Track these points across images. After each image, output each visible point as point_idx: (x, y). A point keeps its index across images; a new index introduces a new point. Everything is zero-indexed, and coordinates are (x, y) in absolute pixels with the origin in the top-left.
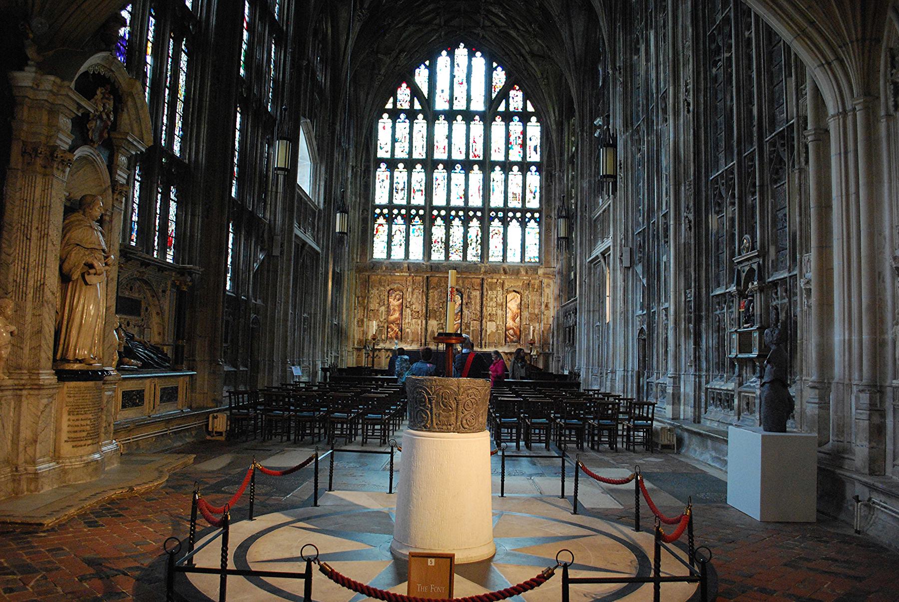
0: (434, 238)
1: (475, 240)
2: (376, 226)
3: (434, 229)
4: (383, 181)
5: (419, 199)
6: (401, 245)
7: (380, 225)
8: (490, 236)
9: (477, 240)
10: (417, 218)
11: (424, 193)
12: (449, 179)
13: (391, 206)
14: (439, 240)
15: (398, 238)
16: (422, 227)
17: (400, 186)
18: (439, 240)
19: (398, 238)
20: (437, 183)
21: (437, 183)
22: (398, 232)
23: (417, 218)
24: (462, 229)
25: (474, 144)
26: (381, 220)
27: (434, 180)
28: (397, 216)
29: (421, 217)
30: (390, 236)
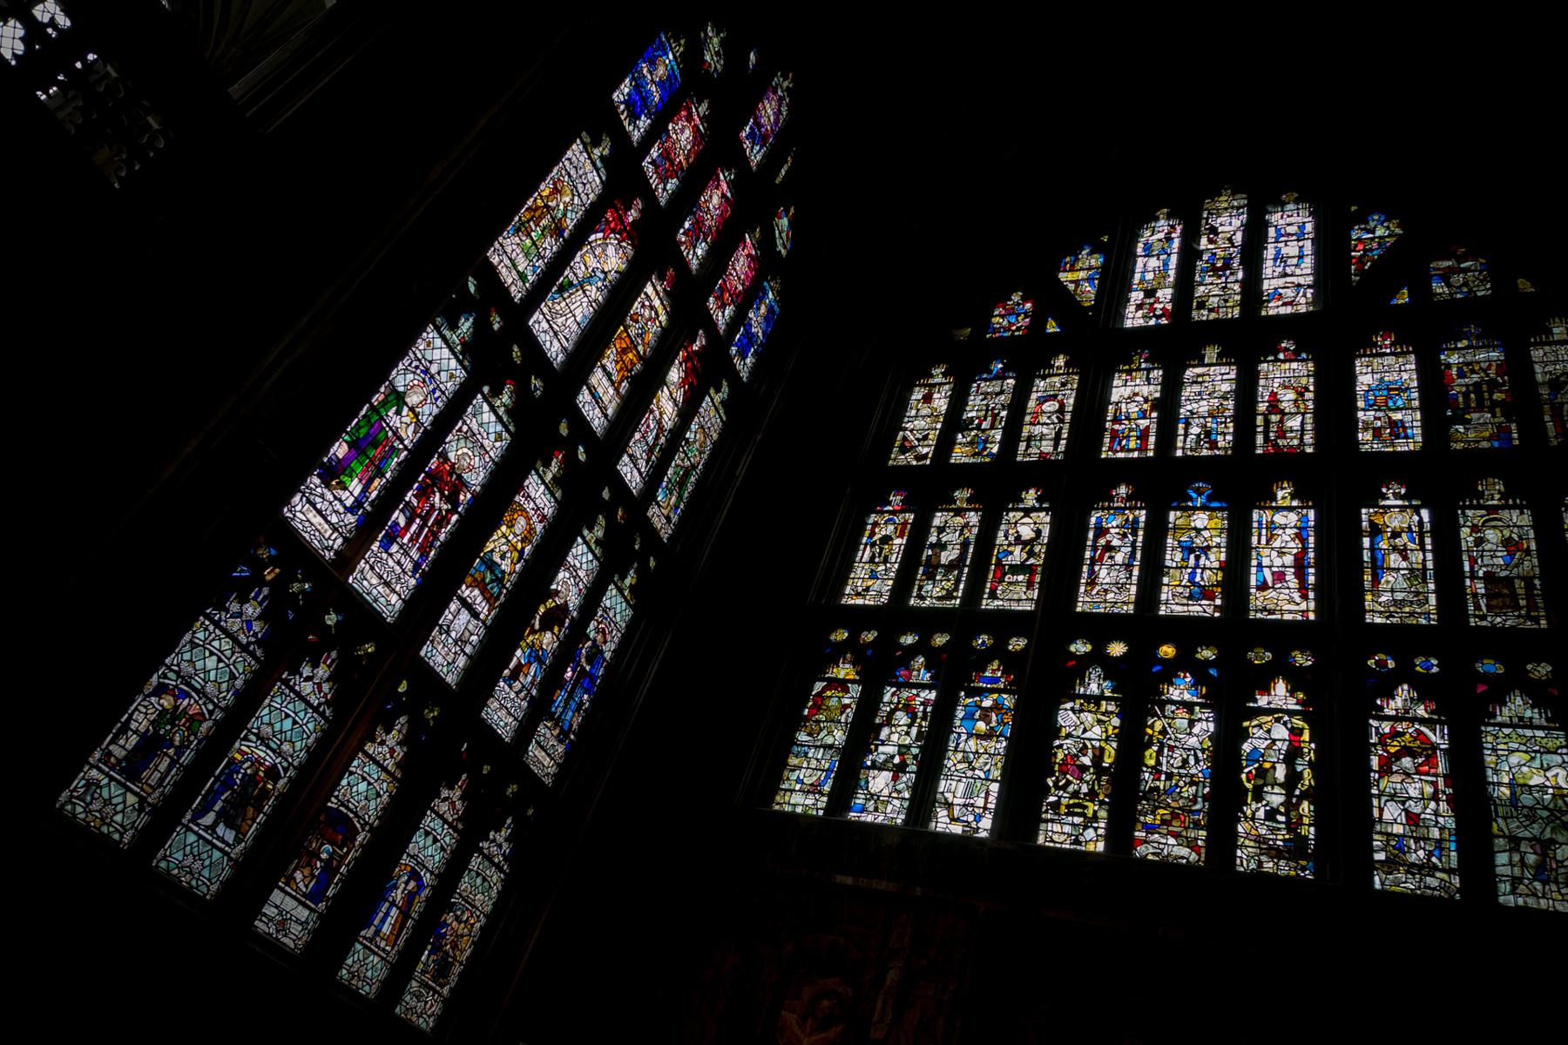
0: (1064, 748)
1: (1281, 773)
2: (819, 686)
3: (1067, 717)
4: (886, 540)
5: (1018, 596)
6: (900, 769)
7: (842, 685)
8: (1375, 762)
9: (1293, 778)
10: (993, 669)
11: (1038, 578)
12: (1157, 532)
13: (895, 614)
14: (1086, 761)
15: (897, 737)
16: (1008, 701)
17: (947, 557)
18: (1086, 761)
19: (897, 737)
20: (1102, 542)
21: (1102, 542)
22: (902, 718)
23: (993, 669)
24: (1206, 726)
25: (1274, 418)
26: (844, 671)
27: (1091, 535)
28: (912, 651)
29: (1011, 663)
30: (864, 732)
